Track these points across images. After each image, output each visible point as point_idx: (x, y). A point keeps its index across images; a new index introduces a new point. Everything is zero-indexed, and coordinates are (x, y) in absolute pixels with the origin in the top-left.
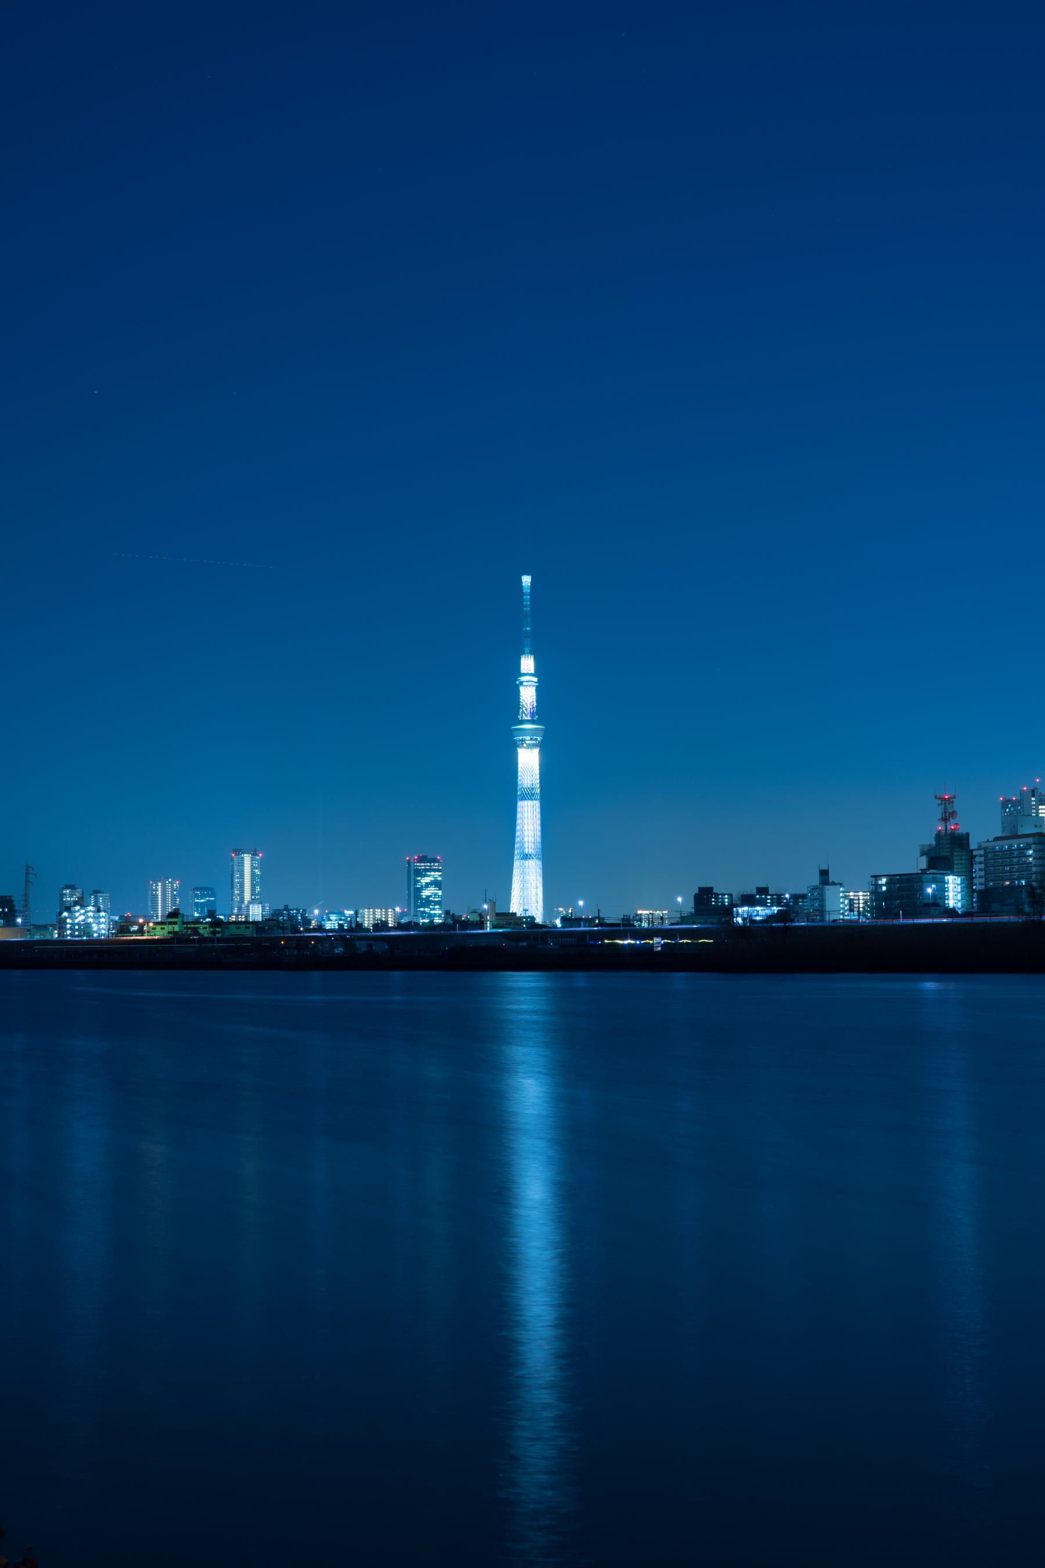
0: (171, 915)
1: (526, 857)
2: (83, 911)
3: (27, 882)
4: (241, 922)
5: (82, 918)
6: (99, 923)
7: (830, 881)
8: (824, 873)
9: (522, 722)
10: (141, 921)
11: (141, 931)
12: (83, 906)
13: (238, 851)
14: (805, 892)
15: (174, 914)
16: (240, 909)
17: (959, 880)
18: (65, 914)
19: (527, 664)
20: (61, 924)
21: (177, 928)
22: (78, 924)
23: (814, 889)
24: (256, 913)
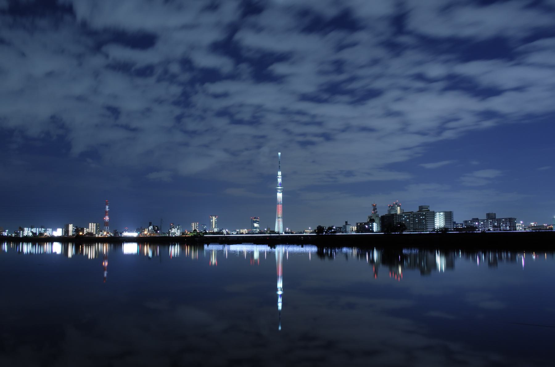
0: (194, 231)
1: (279, 218)
2: (174, 230)
3: (161, 222)
4: (210, 233)
5: (174, 231)
6: (178, 232)
7: (348, 224)
8: (346, 222)
9: (278, 186)
10: (187, 232)
11: (187, 235)
12: (174, 228)
13: (212, 216)
14: (342, 226)
15: (195, 230)
16: (212, 229)
17: (376, 224)
18: (170, 230)
19: (280, 173)
20: (169, 233)
21: (195, 234)
22: (173, 233)
23: (344, 226)
24: (216, 230)
